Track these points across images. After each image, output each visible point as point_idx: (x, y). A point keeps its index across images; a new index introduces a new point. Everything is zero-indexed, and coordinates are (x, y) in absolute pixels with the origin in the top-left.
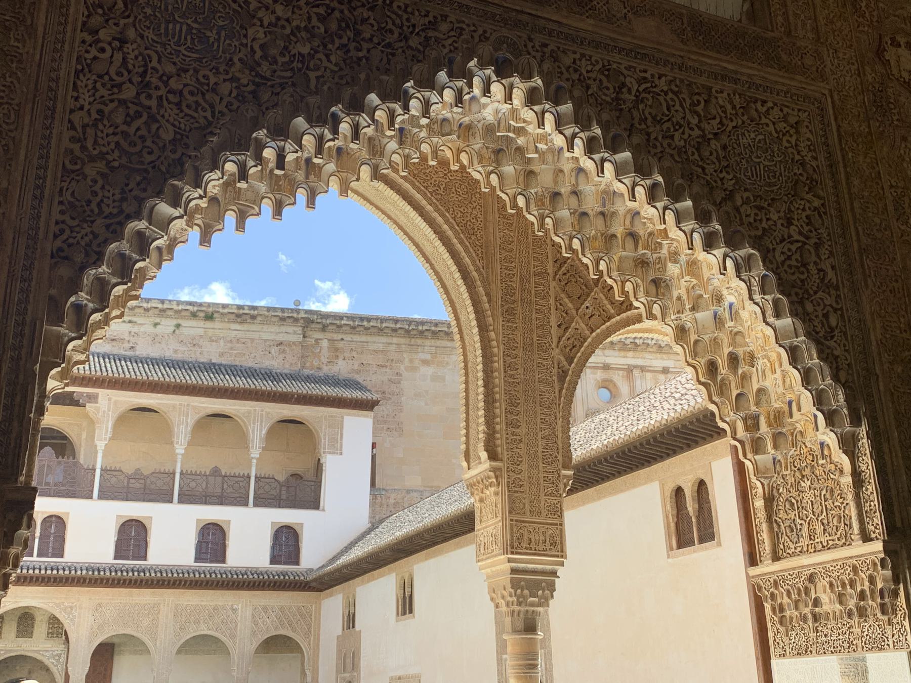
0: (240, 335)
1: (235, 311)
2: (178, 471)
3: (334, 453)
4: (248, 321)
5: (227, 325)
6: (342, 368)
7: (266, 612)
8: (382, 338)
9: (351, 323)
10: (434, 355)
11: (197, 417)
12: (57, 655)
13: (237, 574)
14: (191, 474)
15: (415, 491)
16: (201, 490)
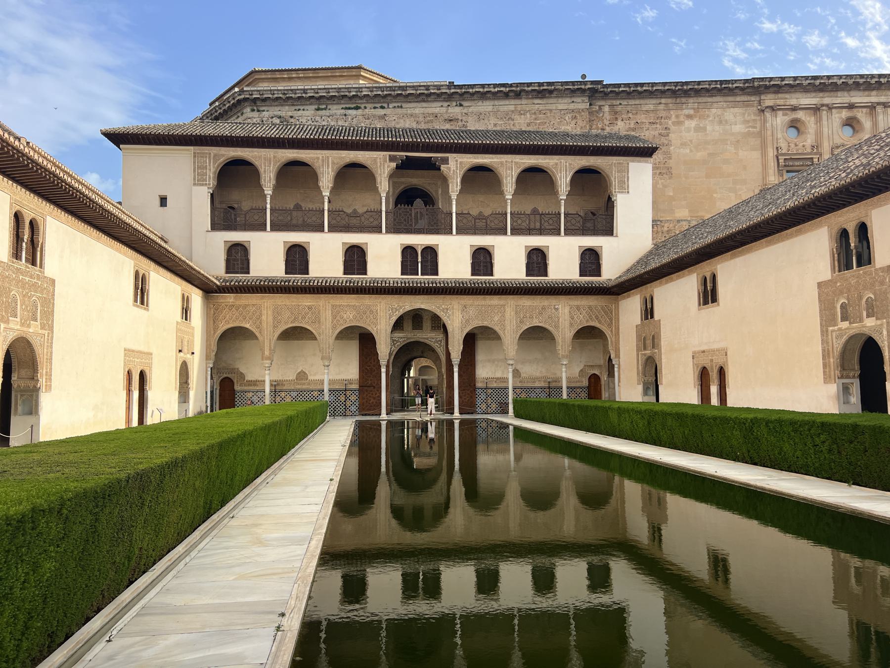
0: (541, 107)
1: (537, 88)
2: (509, 211)
3: (622, 192)
4: (547, 95)
5: (530, 101)
6: (621, 127)
7: (579, 310)
8: (651, 100)
9: (627, 89)
10: (696, 110)
11: (519, 170)
12: (439, 341)
13: (557, 284)
14: (518, 214)
15: (684, 220)
16: (526, 225)
